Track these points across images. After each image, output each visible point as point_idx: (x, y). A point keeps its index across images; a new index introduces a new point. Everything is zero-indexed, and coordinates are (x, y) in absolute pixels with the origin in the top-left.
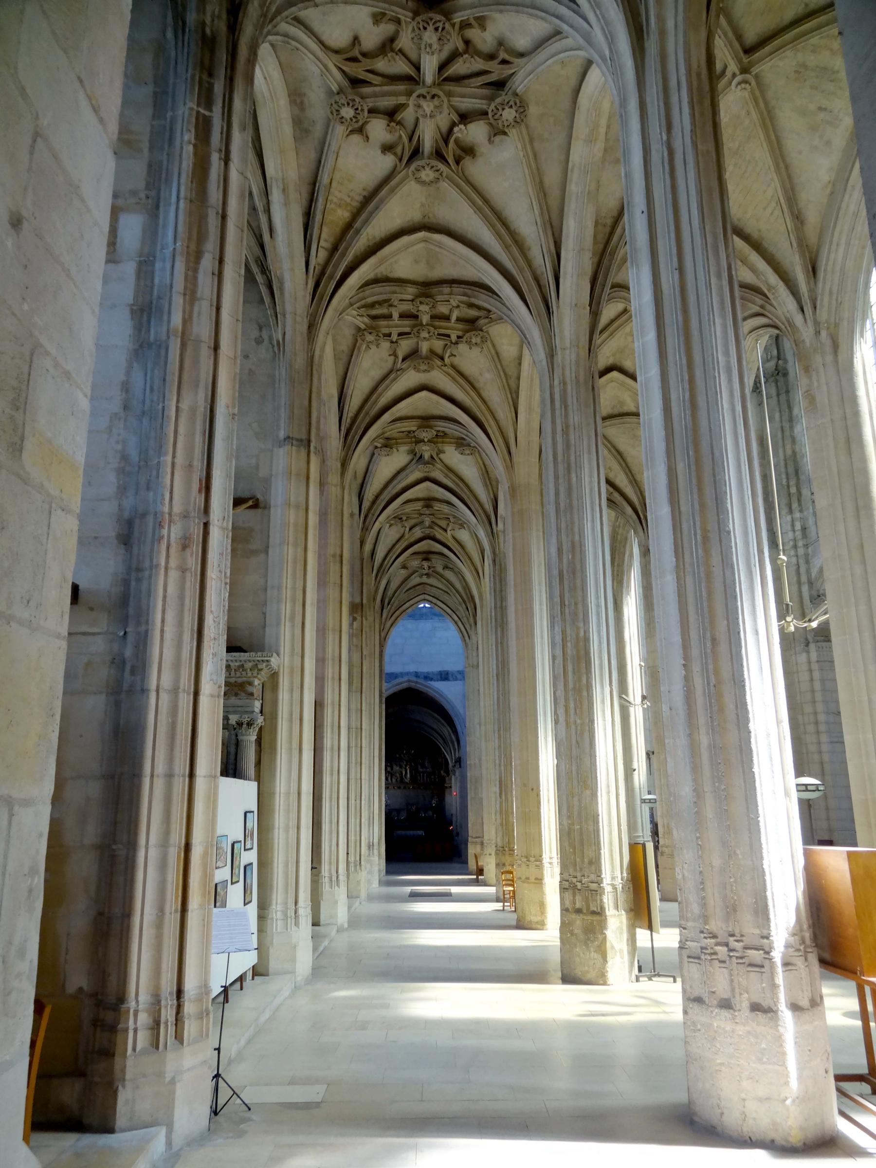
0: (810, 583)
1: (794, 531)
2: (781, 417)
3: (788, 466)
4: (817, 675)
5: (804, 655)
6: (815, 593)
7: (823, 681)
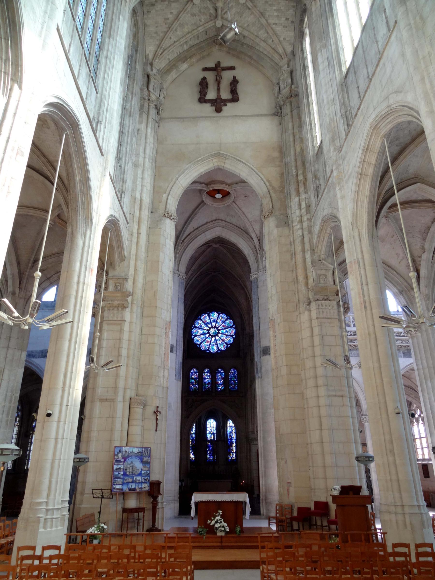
0: (313, 250)
1: (300, 209)
2: (293, 125)
3: (298, 160)
4: (316, 331)
5: (306, 313)
6: (316, 258)
7: (322, 336)
